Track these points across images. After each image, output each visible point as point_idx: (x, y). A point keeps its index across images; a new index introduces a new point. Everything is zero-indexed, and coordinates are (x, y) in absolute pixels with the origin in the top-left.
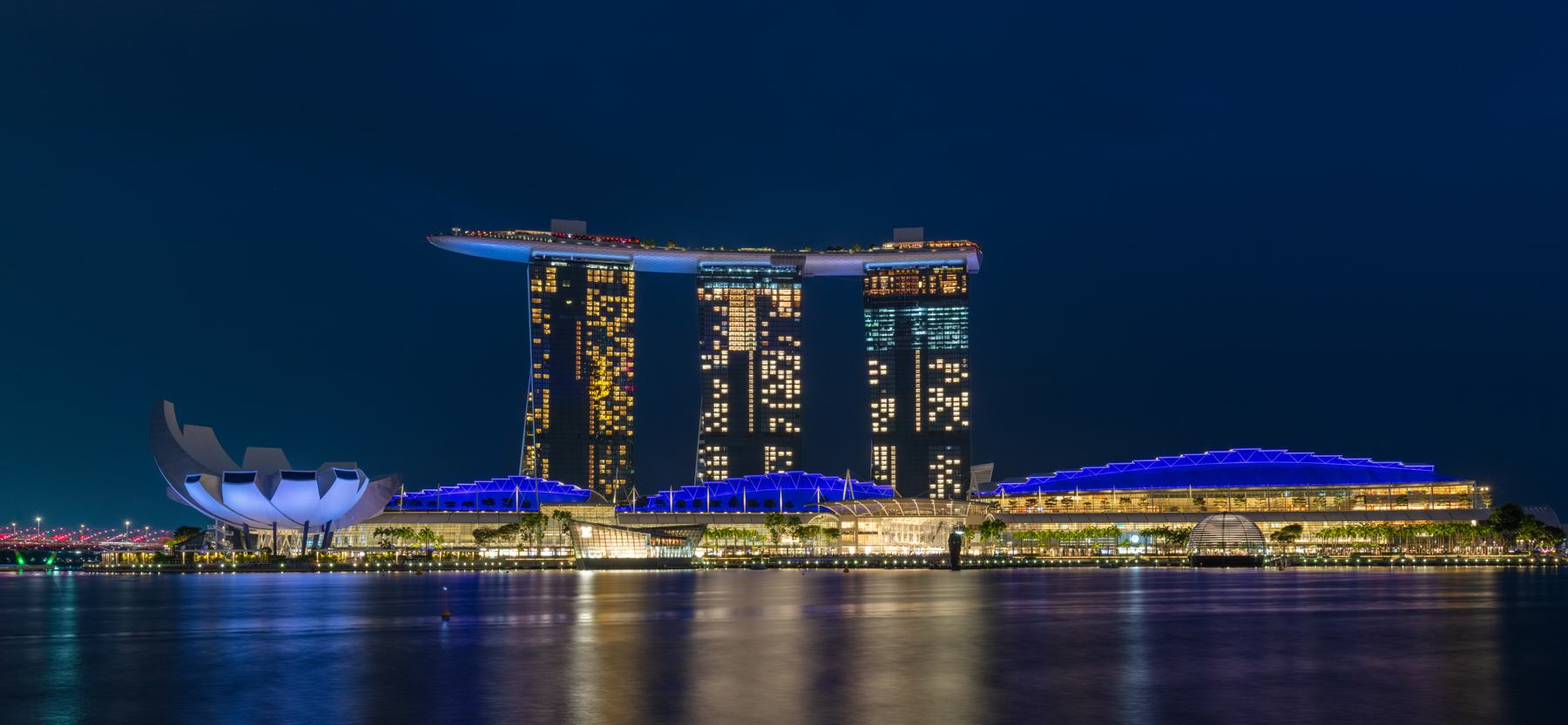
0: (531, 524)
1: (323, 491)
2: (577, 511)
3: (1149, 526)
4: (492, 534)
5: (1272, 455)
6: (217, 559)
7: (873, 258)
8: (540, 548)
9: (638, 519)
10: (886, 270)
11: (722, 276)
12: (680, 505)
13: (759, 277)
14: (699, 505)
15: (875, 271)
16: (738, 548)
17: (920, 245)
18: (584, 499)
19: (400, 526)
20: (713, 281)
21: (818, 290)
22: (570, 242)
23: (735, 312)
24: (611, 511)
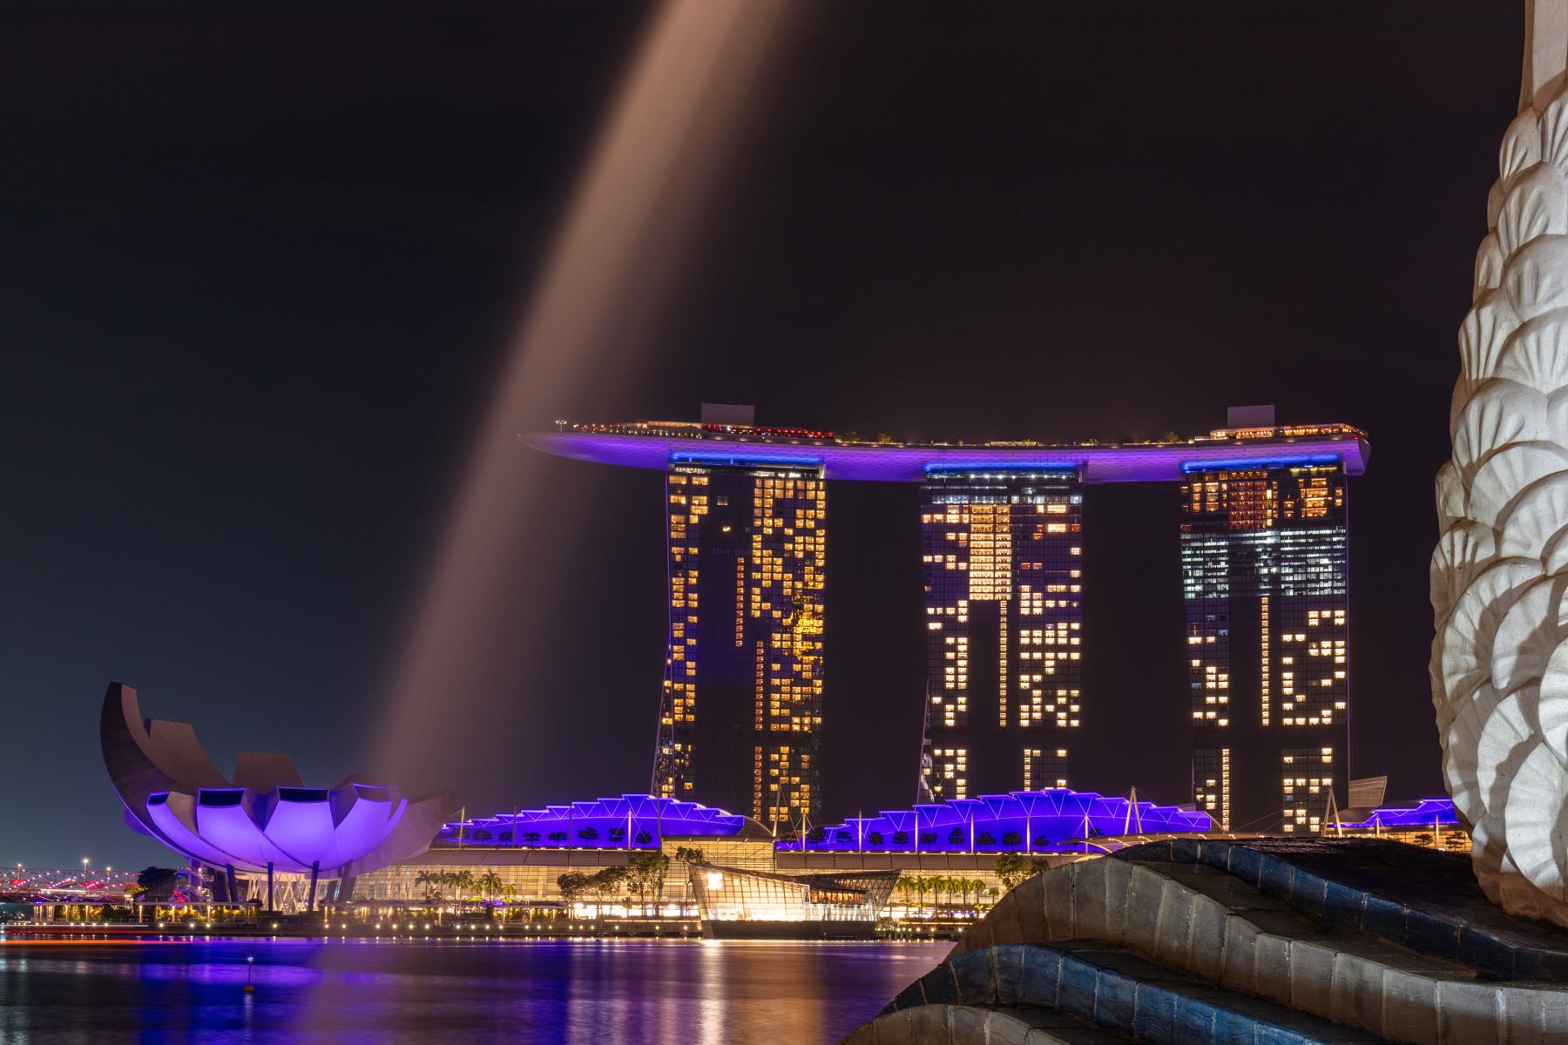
0: (643, 868)
1: (338, 818)
2: (712, 848)
4: (589, 881)
6: (188, 917)
7: (1193, 454)
8: (657, 905)
9: (806, 861)
10: (1215, 472)
11: (960, 485)
12: (874, 841)
13: (1016, 487)
14: (903, 841)
15: (1199, 474)
16: (957, 907)
17: (1266, 432)
18: (733, 831)
19: (457, 870)
21: (1105, 505)
23: (979, 541)
24: (767, 849)
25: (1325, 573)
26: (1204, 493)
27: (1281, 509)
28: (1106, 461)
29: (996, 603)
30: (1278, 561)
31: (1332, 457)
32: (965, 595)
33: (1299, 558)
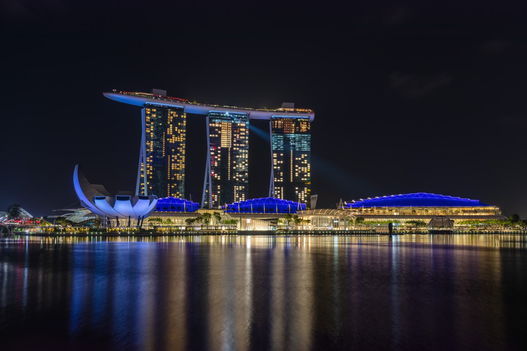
3: (409, 220)
5: (429, 195)
7: (276, 113)
10: (280, 119)
13: (232, 119)
20: (215, 119)
23: (224, 132)
25: (305, 146)
26: (278, 123)
27: (296, 129)
28: (257, 114)
29: (227, 148)
30: (295, 142)
31: (307, 117)
32: (220, 146)
33: (300, 141)
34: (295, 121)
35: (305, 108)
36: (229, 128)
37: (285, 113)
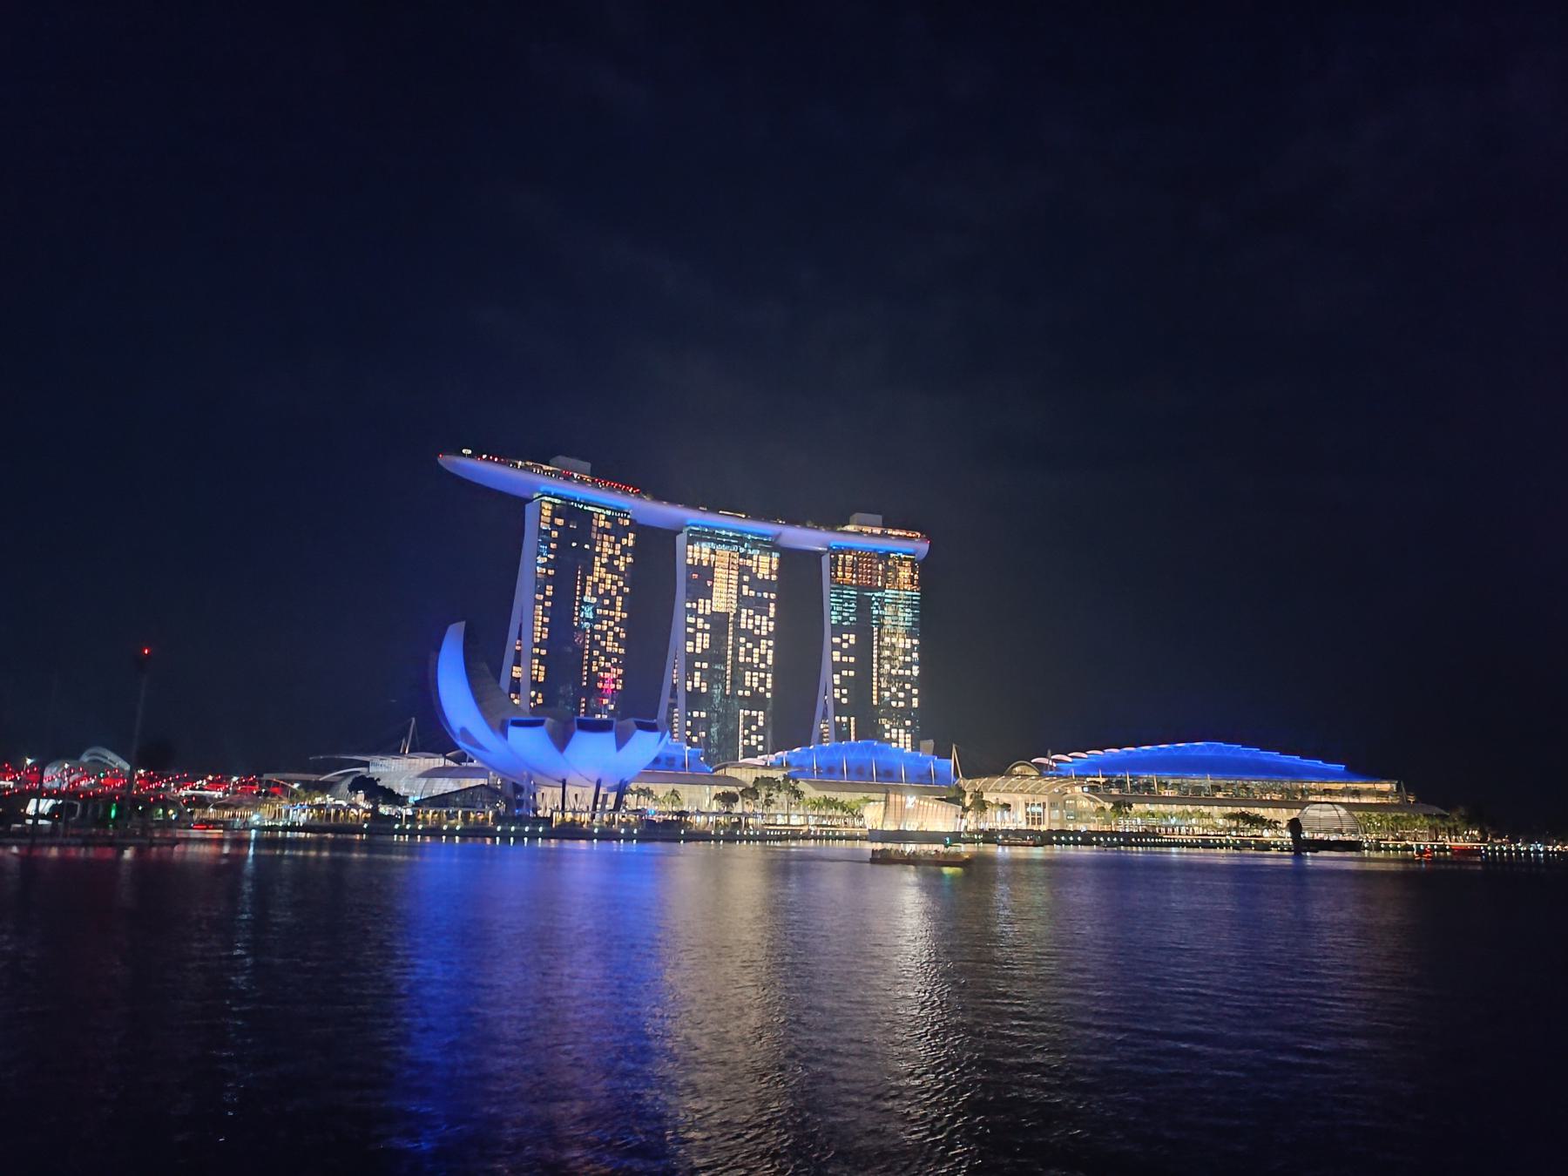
7: (840, 536)
10: (850, 550)
20: (701, 540)
22: (581, 481)
34: (885, 556)
35: (907, 529)
36: (728, 567)
37: (861, 535)
